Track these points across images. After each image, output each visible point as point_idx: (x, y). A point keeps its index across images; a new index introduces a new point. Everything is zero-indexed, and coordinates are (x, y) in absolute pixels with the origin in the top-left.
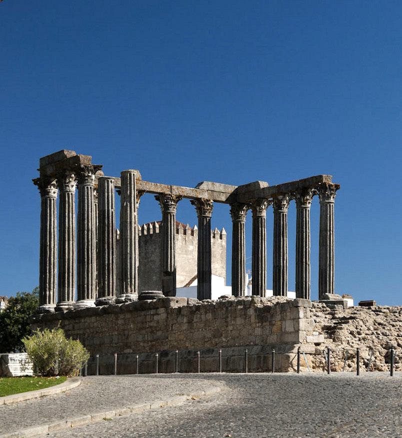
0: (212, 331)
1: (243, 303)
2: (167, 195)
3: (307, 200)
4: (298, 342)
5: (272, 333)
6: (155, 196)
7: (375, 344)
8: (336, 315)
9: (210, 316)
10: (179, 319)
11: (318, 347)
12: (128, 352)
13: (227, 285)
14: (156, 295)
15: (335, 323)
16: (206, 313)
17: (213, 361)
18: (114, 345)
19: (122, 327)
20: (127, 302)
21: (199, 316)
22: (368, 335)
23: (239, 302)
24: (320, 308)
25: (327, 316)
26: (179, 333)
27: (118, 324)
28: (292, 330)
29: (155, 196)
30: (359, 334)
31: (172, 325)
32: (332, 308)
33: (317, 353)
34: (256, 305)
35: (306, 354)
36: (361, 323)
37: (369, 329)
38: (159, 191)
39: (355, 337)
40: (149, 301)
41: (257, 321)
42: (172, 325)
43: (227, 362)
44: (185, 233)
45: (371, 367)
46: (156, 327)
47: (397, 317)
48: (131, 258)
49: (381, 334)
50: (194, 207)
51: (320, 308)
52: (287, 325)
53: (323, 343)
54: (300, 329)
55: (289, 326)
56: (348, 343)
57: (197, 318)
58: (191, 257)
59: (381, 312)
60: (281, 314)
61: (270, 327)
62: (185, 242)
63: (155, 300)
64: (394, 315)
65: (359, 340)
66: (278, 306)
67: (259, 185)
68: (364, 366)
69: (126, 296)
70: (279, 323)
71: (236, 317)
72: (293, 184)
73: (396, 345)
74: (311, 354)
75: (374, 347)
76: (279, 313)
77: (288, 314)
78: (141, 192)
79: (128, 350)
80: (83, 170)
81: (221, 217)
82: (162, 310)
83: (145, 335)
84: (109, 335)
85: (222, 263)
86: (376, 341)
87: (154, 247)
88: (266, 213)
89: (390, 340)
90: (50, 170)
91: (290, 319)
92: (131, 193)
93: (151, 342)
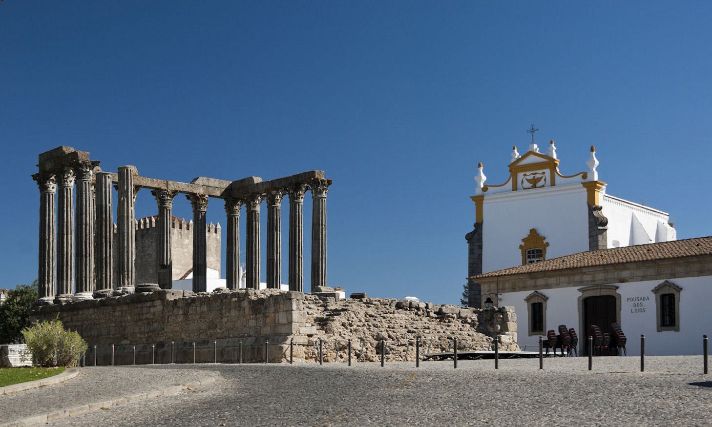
0: (208, 323)
1: (237, 295)
2: (163, 190)
3: (300, 195)
4: (291, 334)
5: (265, 325)
6: (152, 191)
7: (367, 335)
8: (328, 308)
9: (205, 308)
10: (175, 311)
11: (311, 339)
12: (126, 343)
13: (222, 278)
14: (152, 287)
15: (327, 315)
16: (201, 305)
17: (208, 351)
18: (112, 336)
19: (119, 319)
20: (124, 294)
21: (194, 308)
22: (360, 326)
23: (234, 295)
24: (312, 300)
25: (320, 308)
26: (175, 325)
27: (115, 316)
28: (285, 321)
29: (152, 191)
30: (351, 325)
31: (168, 317)
32: (325, 300)
33: (310, 344)
34: (250, 297)
35: (299, 345)
36: (353, 315)
37: (360, 321)
38: (155, 186)
39: (347, 329)
40: (146, 293)
41: (251, 313)
42: (168, 317)
43: (222, 353)
44: (181, 228)
45: (363, 357)
46: (152, 319)
47: (388, 309)
48: (128, 252)
49: (372, 326)
50: (190, 201)
51: (312, 300)
53: (316, 334)
54: (293, 320)
55: (282, 318)
56: (340, 335)
57: (192, 310)
58: (187, 250)
59: (372, 304)
60: (274, 306)
61: (263, 319)
62: (181, 236)
63: (151, 293)
64: (385, 307)
65: (351, 332)
66: (271, 299)
67: (253, 180)
68: (356, 357)
69: (123, 289)
70: (273, 315)
71: (230, 309)
72: (286, 179)
73: (386, 336)
74: (303, 345)
75: (365, 339)
77: (281, 306)
78: (137, 187)
79: (126, 341)
80: (81, 165)
81: (215, 211)
82: (158, 303)
83: (141, 326)
84: (107, 327)
85: (216, 256)
86: (367, 332)
87: (151, 241)
88: (260, 208)
89: (381, 332)
90: (48, 166)
91: (283, 311)
92: (128, 188)
93: (148, 333)
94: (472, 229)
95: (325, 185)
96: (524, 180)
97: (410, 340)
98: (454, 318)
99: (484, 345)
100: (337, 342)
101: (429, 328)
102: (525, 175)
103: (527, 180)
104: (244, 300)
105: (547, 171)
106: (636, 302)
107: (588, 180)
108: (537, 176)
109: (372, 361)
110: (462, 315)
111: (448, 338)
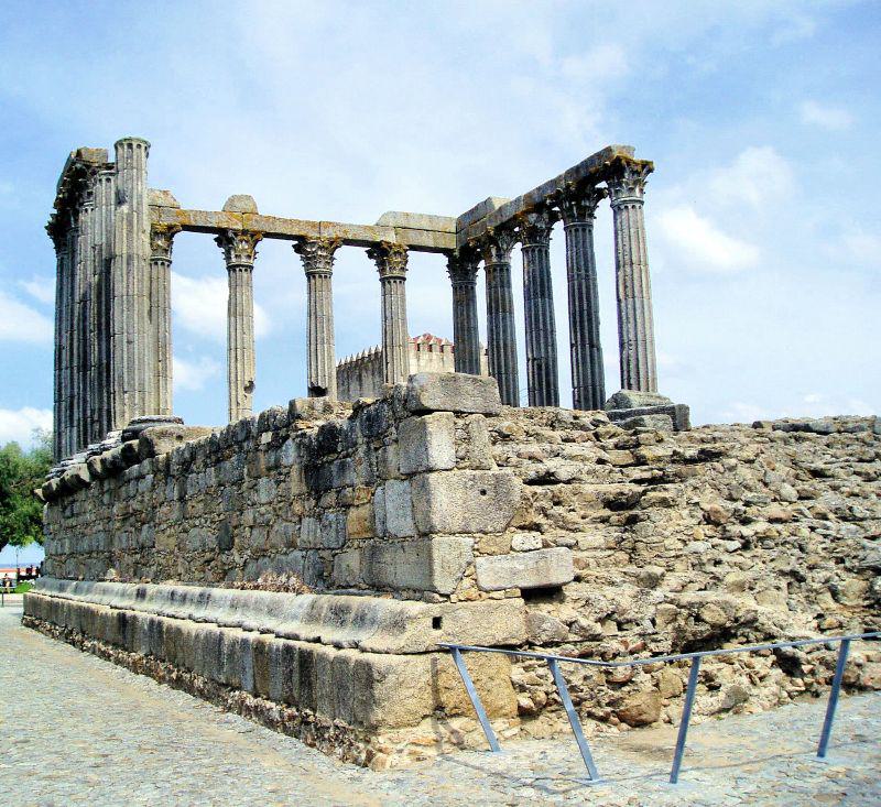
6: (294, 246)
7: (813, 559)
11: (544, 609)
15: (639, 482)
16: (206, 466)
24: (583, 428)
25: (610, 456)
29: (294, 246)
41: (305, 489)
49: (831, 516)
50: (374, 261)
51: (583, 428)
52: (389, 506)
53: (578, 579)
60: (368, 453)
75: (809, 575)
76: (361, 450)
95: (639, 173)
100: (685, 612)
104: (286, 438)
109: (863, 689)
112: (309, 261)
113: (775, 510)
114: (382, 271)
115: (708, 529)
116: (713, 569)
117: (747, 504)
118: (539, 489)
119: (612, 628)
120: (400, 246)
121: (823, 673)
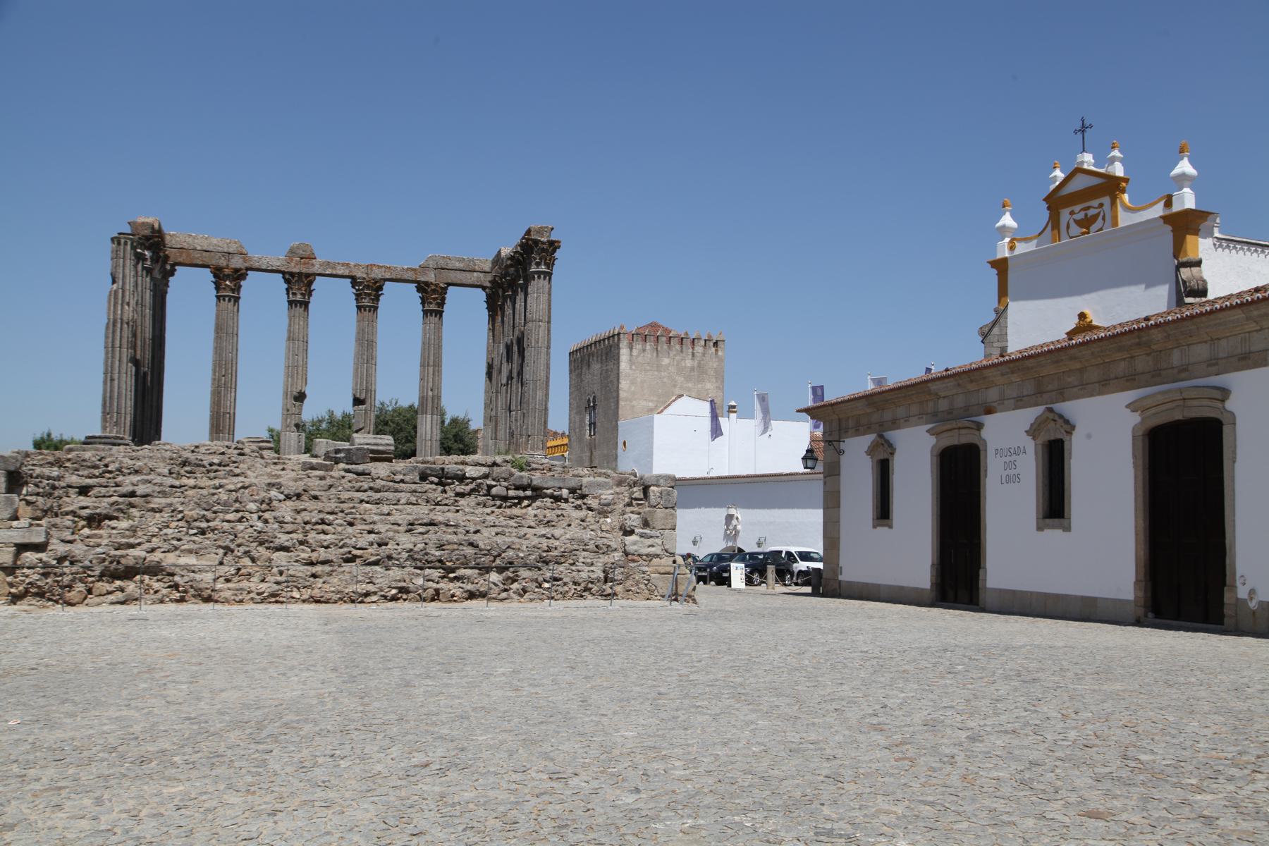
7: (239, 541)
81: (467, 310)
94: (993, 316)
96: (1071, 222)
97: (355, 552)
98: (557, 499)
99: (581, 560)
101: (432, 524)
102: (1072, 213)
103: (1076, 221)
105: (1106, 200)
106: (1008, 459)
107: (1176, 208)
108: (1092, 212)
109: (208, 600)
110: (585, 491)
111: (471, 544)
112: (358, 297)
113: (230, 517)
114: (423, 303)
115: (181, 524)
116: (175, 542)
117: (215, 512)
118: (121, 500)
119: (67, 563)
120: (436, 285)
121: (192, 592)
